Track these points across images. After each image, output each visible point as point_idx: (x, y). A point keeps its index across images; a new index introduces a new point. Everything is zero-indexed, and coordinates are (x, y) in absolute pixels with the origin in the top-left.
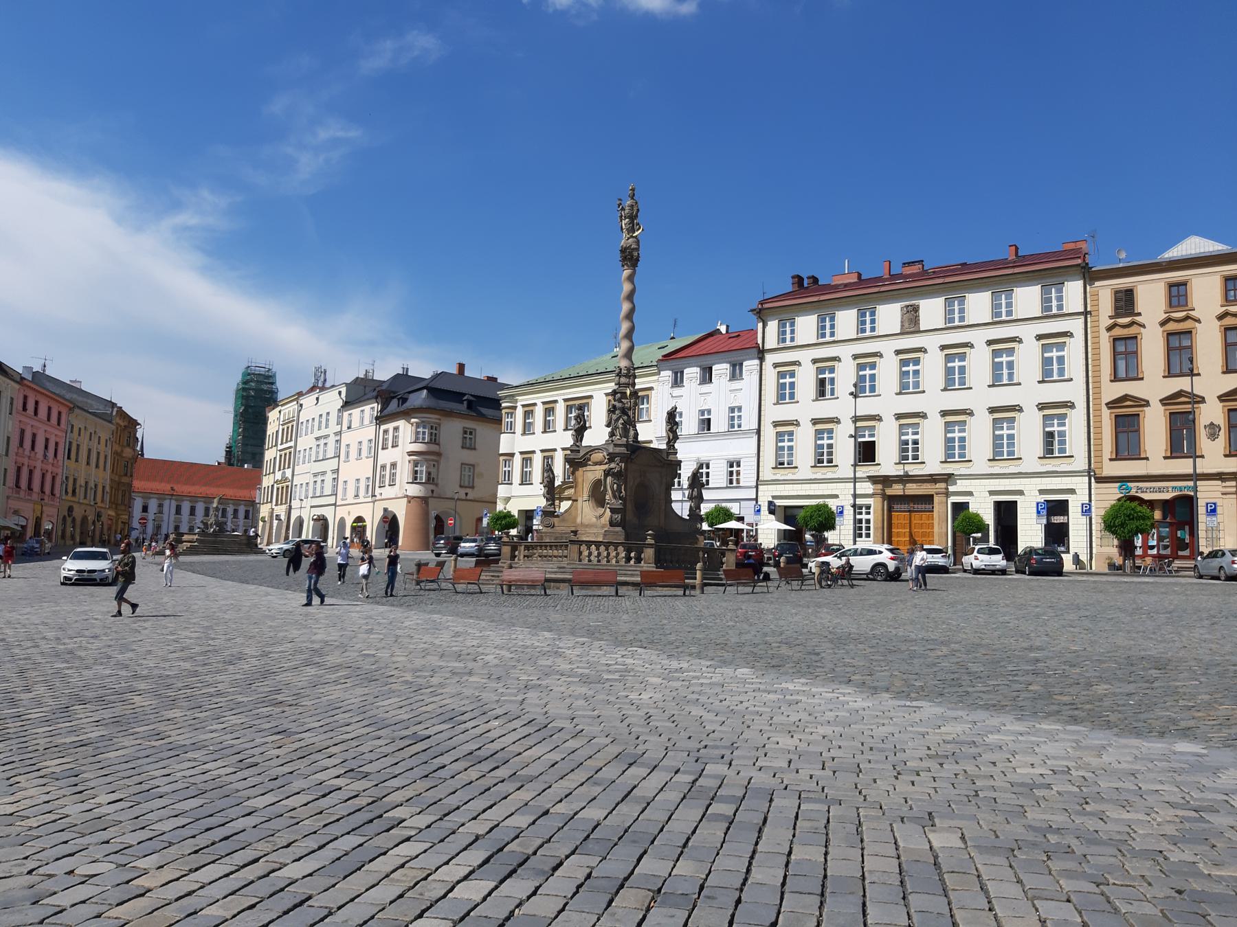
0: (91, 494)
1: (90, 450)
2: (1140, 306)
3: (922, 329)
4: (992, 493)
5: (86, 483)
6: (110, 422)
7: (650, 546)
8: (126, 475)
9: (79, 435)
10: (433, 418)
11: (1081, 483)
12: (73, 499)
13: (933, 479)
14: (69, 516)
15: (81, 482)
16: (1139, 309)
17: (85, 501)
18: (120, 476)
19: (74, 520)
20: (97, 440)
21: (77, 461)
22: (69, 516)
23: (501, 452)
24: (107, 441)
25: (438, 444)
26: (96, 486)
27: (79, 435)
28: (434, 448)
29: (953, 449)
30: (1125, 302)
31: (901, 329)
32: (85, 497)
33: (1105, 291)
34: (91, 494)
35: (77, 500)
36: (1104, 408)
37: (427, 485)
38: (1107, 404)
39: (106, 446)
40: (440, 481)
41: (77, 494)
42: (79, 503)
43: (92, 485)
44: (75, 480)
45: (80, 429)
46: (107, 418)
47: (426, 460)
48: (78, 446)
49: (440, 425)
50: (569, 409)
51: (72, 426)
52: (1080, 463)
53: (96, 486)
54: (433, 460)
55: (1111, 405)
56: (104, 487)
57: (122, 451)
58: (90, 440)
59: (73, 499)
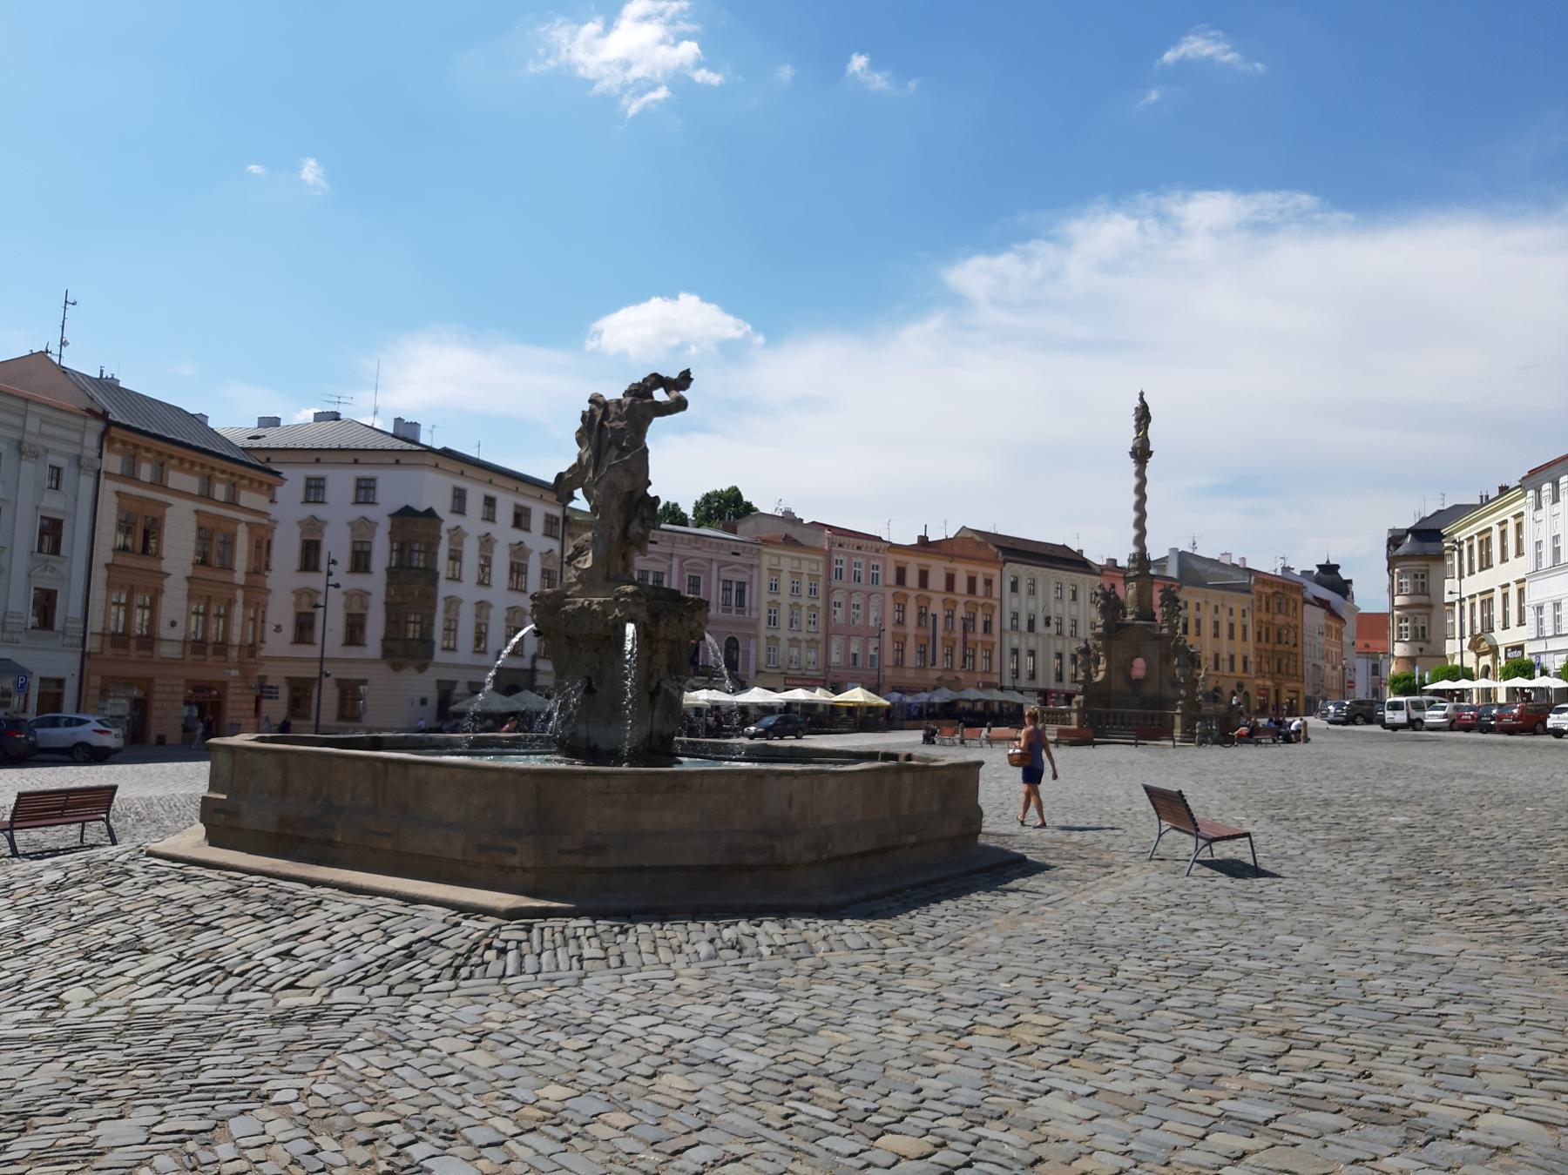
0: (1224, 667)
5: (1217, 656)
6: (1248, 592)
7: (1075, 711)
8: (1279, 642)
9: (1198, 609)
10: (1416, 565)
18: (1273, 644)
20: (1227, 612)
21: (1198, 634)
23: (1446, 601)
25: (1428, 594)
26: (1232, 658)
27: (1198, 609)
28: (1423, 599)
32: (1217, 668)
34: (1224, 667)
37: (1413, 643)
39: (1244, 616)
40: (1432, 637)
41: (1220, 668)
42: (1223, 676)
45: (1198, 605)
46: (1244, 589)
47: (1410, 614)
49: (1428, 571)
50: (1481, 542)
53: (1232, 658)
54: (1425, 614)
56: (1245, 659)
57: (1273, 619)
58: (1216, 612)
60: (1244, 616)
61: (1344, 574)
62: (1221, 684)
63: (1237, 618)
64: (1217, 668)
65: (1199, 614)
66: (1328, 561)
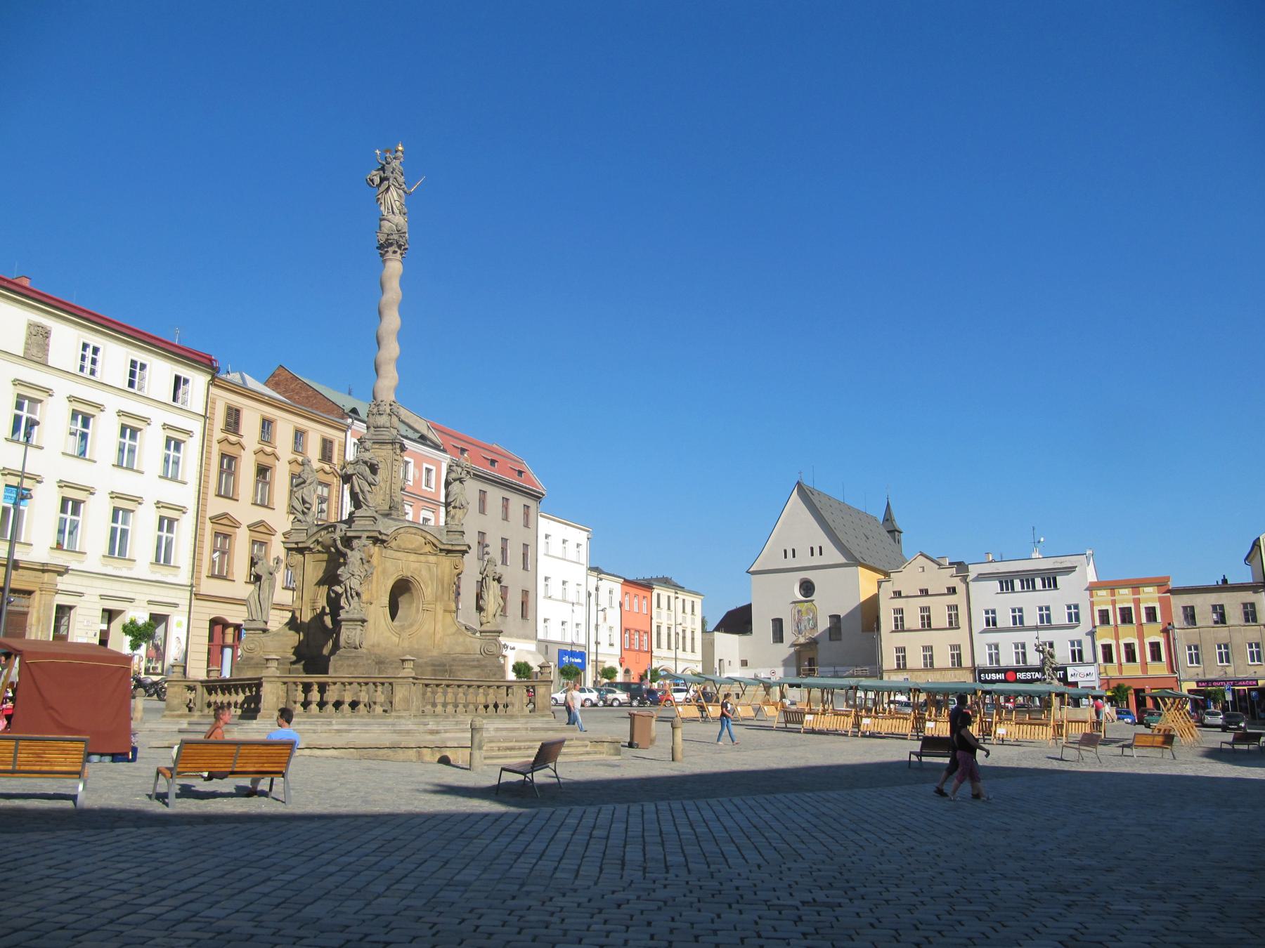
2: (243, 429)
3: (49, 364)
4: (103, 597)
11: (182, 597)
13: (44, 569)
16: (242, 432)
29: (65, 535)
30: (233, 419)
31: (25, 353)
33: (224, 399)
36: (208, 521)
38: (210, 519)
52: (184, 577)
55: (215, 520)
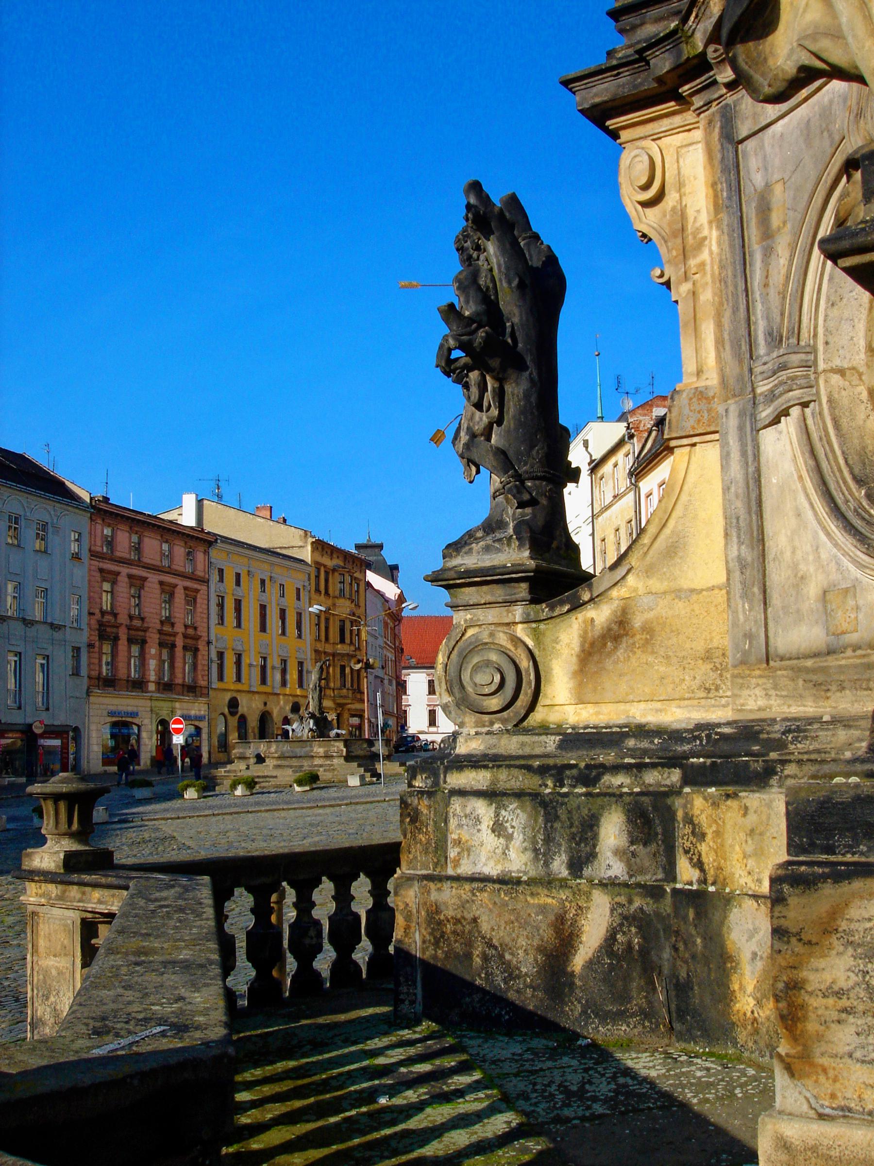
1: (263, 608)
9: (238, 583)
12: (239, 687)
14: (233, 714)
15: (252, 659)
17: (263, 689)
19: (243, 720)
22: (233, 714)
24: (298, 590)
26: (284, 662)
27: (238, 583)
32: (264, 681)
35: (245, 688)
39: (298, 599)
43: (274, 661)
44: (239, 657)
45: (238, 576)
48: (238, 603)
51: (221, 571)
53: (284, 662)
59: (239, 687)
60: (298, 599)
61: (389, 556)
62: (268, 708)
63: (290, 602)
64: (264, 681)
65: (240, 592)
66: (369, 540)
